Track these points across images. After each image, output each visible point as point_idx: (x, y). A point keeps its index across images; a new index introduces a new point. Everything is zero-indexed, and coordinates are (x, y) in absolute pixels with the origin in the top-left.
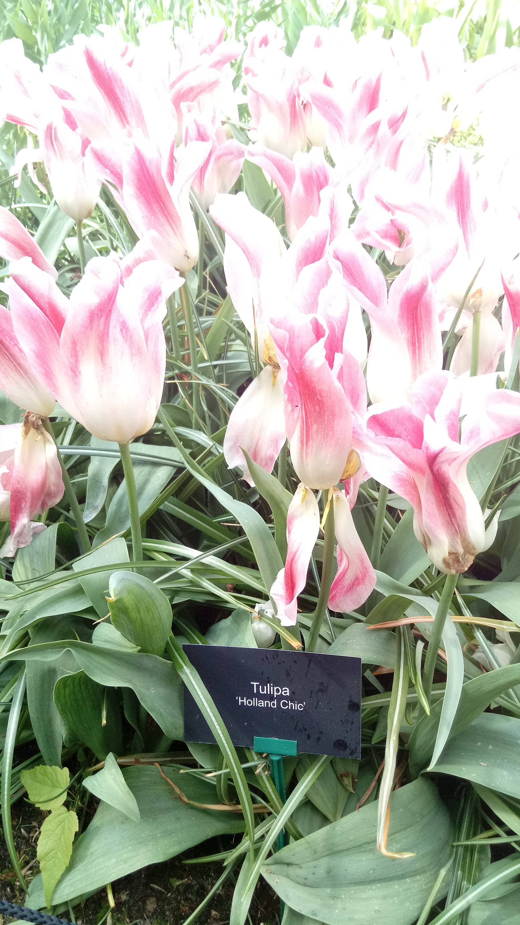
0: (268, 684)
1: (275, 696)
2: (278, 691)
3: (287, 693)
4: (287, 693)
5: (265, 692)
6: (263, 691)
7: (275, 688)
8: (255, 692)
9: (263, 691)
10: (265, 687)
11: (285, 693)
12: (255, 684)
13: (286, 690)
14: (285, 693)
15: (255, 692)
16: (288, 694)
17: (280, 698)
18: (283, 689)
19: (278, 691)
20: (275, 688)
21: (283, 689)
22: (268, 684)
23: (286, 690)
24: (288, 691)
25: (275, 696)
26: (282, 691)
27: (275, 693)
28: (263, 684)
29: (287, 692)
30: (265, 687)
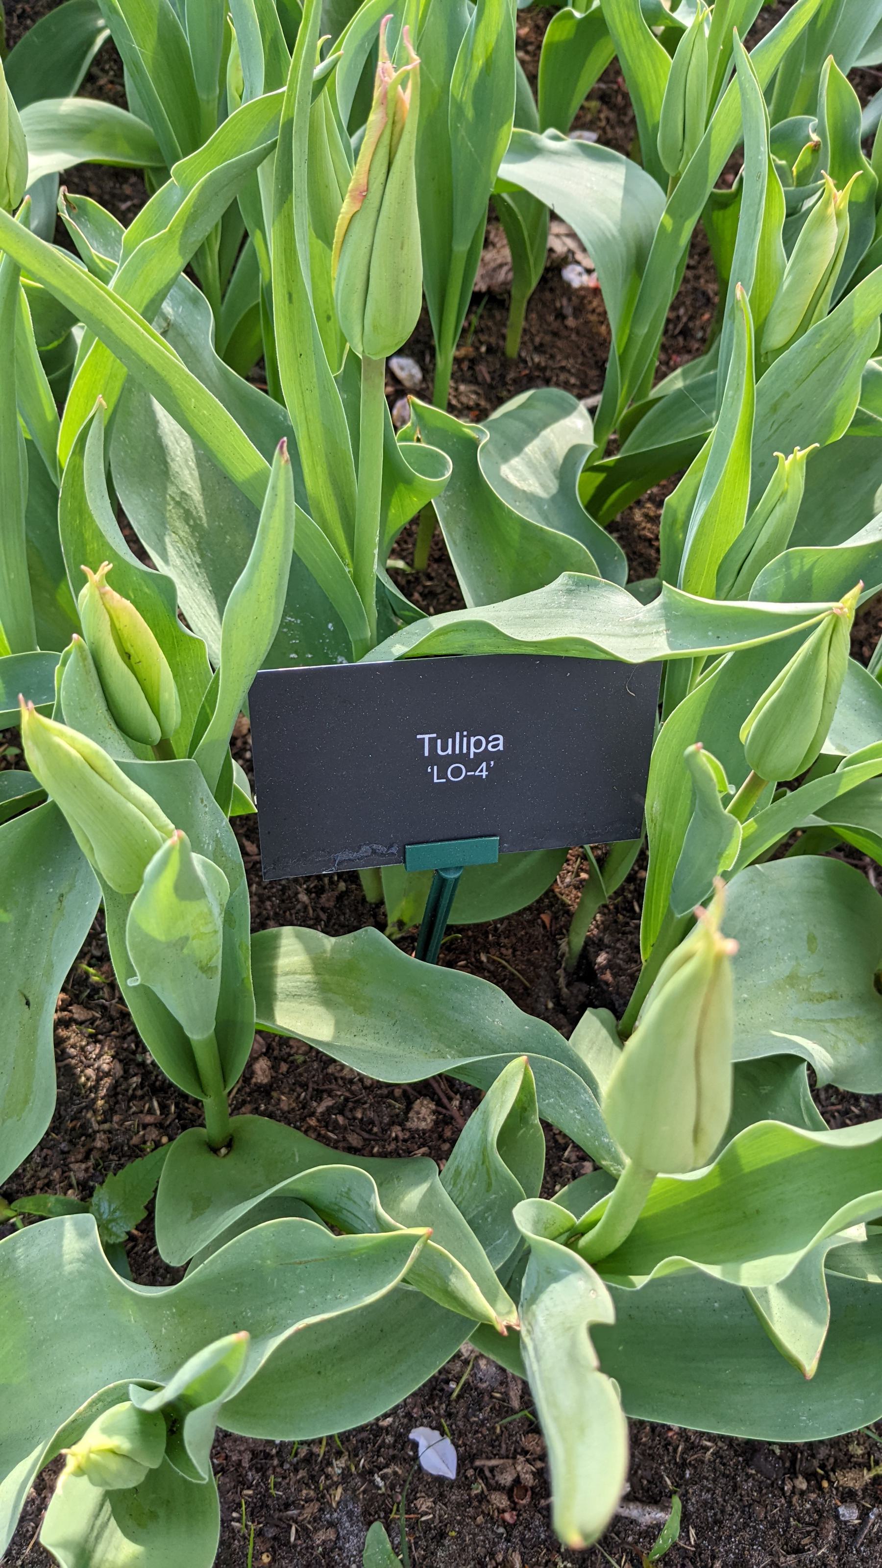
0: (458, 734)
2: (478, 744)
3: (498, 745)
4: (498, 745)
5: (449, 751)
6: (444, 749)
7: (473, 740)
9: (444, 749)
10: (450, 740)
11: (493, 747)
13: (498, 739)
14: (493, 747)
19: (478, 744)
20: (473, 740)
22: (458, 734)
24: (501, 742)
26: (488, 742)
27: (473, 749)
30: (450, 740)
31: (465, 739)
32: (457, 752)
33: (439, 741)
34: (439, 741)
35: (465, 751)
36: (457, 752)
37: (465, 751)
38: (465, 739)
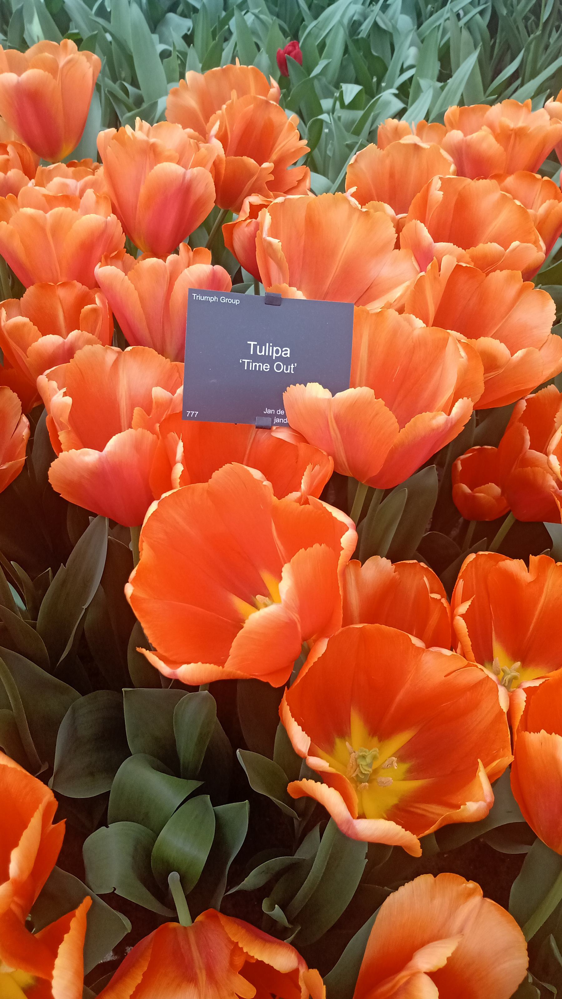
0: (267, 344)
1: (274, 358)
2: (277, 352)
3: (287, 354)
4: (287, 354)
5: (263, 353)
6: (261, 352)
7: (275, 349)
8: (252, 353)
9: (261, 352)
10: (264, 347)
12: (252, 343)
13: (287, 350)
14: (285, 354)
15: (252, 353)
16: (288, 355)
17: (280, 359)
18: (284, 349)
19: (277, 352)
21: (284, 349)
22: (267, 344)
23: (287, 350)
24: (289, 352)
25: (274, 358)
26: (282, 351)
27: (275, 354)
28: (262, 344)
29: (287, 352)
30: (264, 347)
31: (271, 348)
32: (267, 354)
33: (258, 347)
34: (258, 347)
35: (271, 354)
36: (267, 354)
37: (271, 354)
38: (271, 348)
